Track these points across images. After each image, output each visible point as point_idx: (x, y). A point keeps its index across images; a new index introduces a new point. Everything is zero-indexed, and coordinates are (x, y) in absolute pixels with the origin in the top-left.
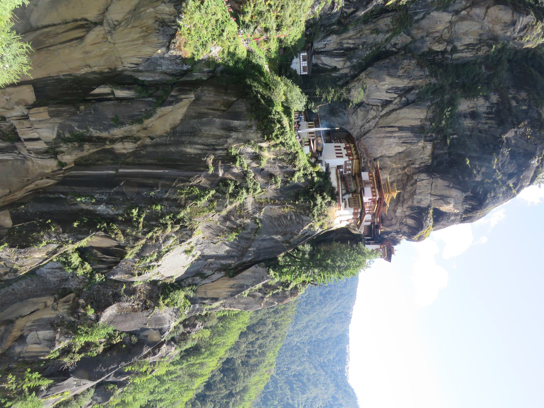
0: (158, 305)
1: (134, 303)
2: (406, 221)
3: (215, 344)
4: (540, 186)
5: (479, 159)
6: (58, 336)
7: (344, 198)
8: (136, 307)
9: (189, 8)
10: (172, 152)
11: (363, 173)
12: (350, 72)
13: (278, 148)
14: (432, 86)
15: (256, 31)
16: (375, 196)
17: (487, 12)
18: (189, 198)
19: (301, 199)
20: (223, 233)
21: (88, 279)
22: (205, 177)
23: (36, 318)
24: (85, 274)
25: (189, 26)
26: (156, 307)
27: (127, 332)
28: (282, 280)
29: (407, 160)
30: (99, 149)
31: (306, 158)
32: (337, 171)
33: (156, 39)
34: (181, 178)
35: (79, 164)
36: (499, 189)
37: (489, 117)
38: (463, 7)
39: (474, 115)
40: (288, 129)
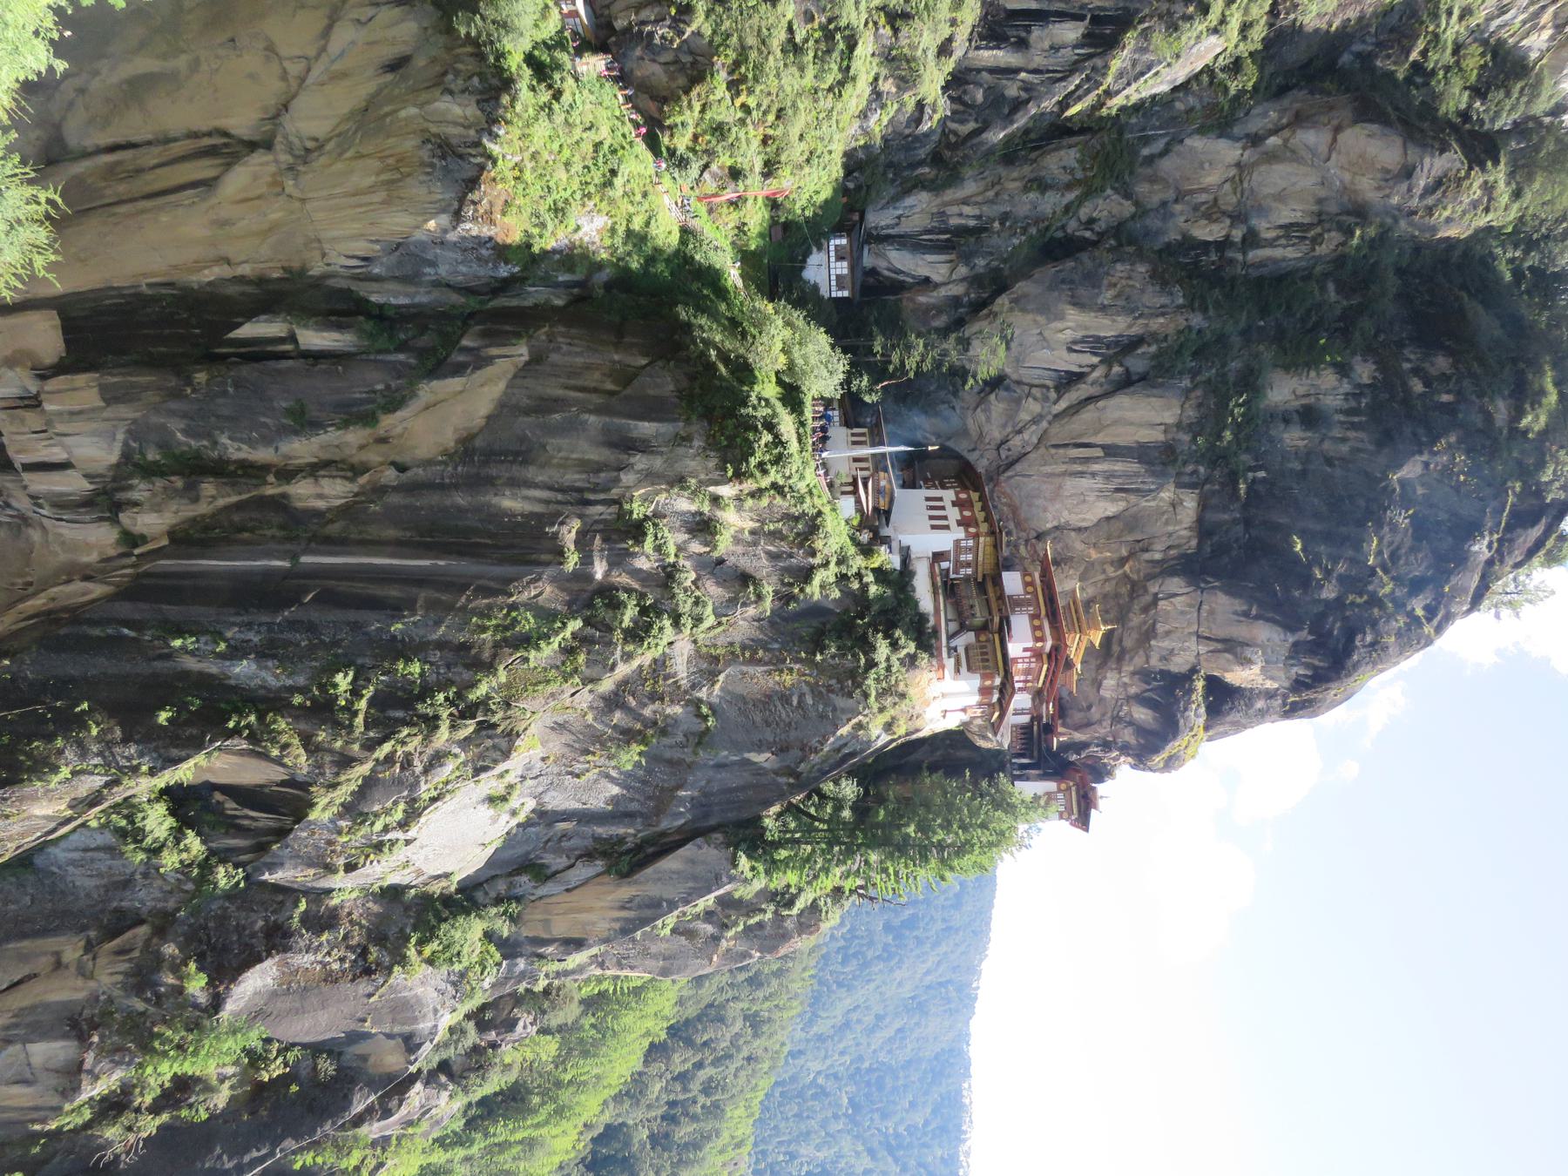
0: (402, 960)
1: (329, 953)
2: (1129, 713)
3: (570, 1082)
4: (1497, 616)
5: (1328, 537)
6: (89, 1058)
7: (953, 644)
8: (336, 966)
9: (518, 108)
10: (460, 509)
11: (1005, 575)
12: (967, 294)
13: (765, 502)
14: (1193, 336)
15: (706, 175)
16: (1042, 639)
17: (1335, 140)
18: (506, 642)
19: (829, 647)
20: (603, 745)
21: (194, 880)
22: (553, 580)
23: (26, 1003)
24: (185, 867)
25: (517, 159)
26: (397, 969)
27: (304, 1046)
28: (772, 886)
29: (1130, 538)
30: (244, 497)
31: (844, 530)
32: (932, 567)
33: (423, 191)
34: (481, 582)
35: (184, 539)
36: (1388, 621)
37: (1353, 424)
38: (1270, 126)
39: (1309, 416)
40: (794, 446)
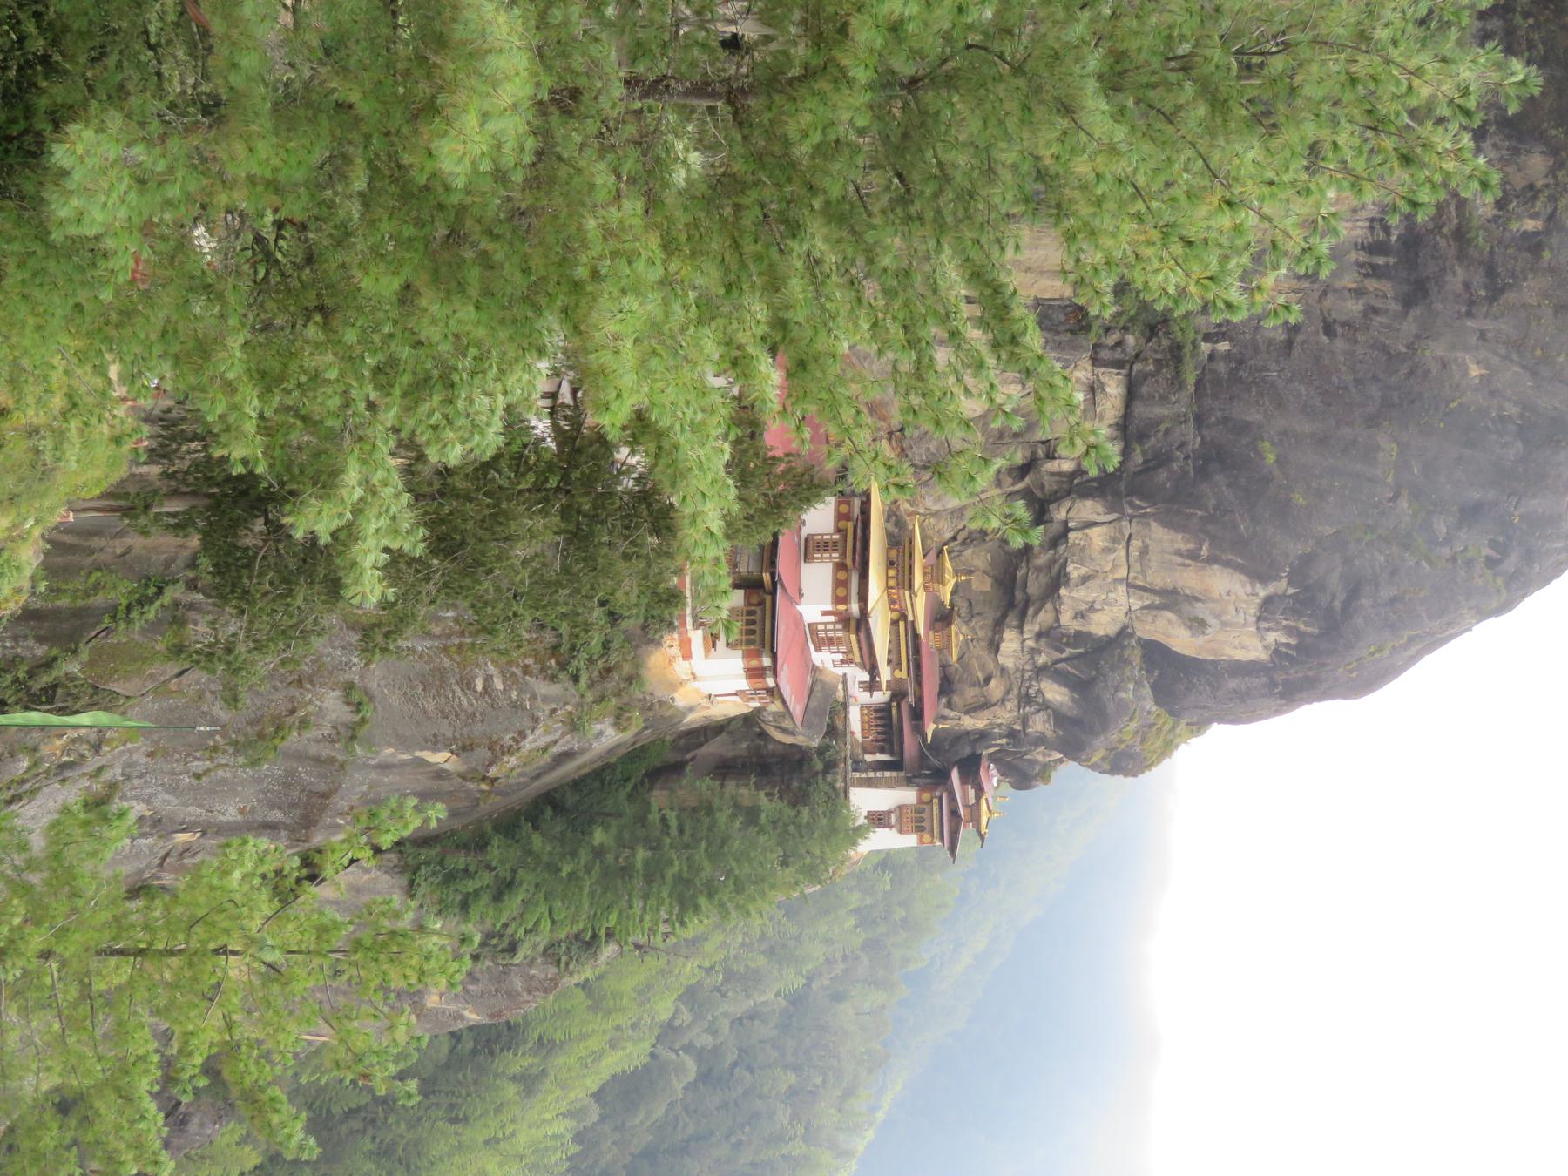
2: (1039, 691)
37: (1374, 267)
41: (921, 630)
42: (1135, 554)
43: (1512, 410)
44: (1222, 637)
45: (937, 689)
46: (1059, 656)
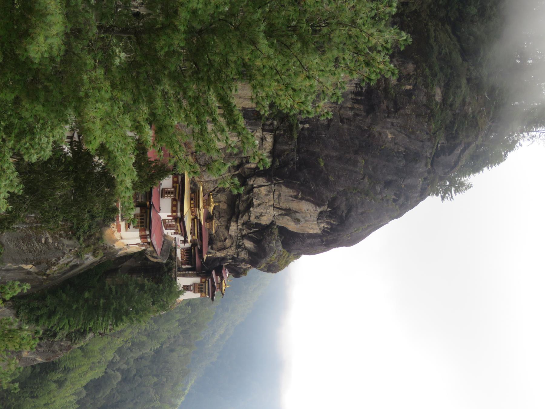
2: (243, 244)
37: (357, 100)
41: (202, 222)
42: (276, 196)
43: (402, 149)
44: (305, 225)
45: (208, 242)
46: (249, 231)
